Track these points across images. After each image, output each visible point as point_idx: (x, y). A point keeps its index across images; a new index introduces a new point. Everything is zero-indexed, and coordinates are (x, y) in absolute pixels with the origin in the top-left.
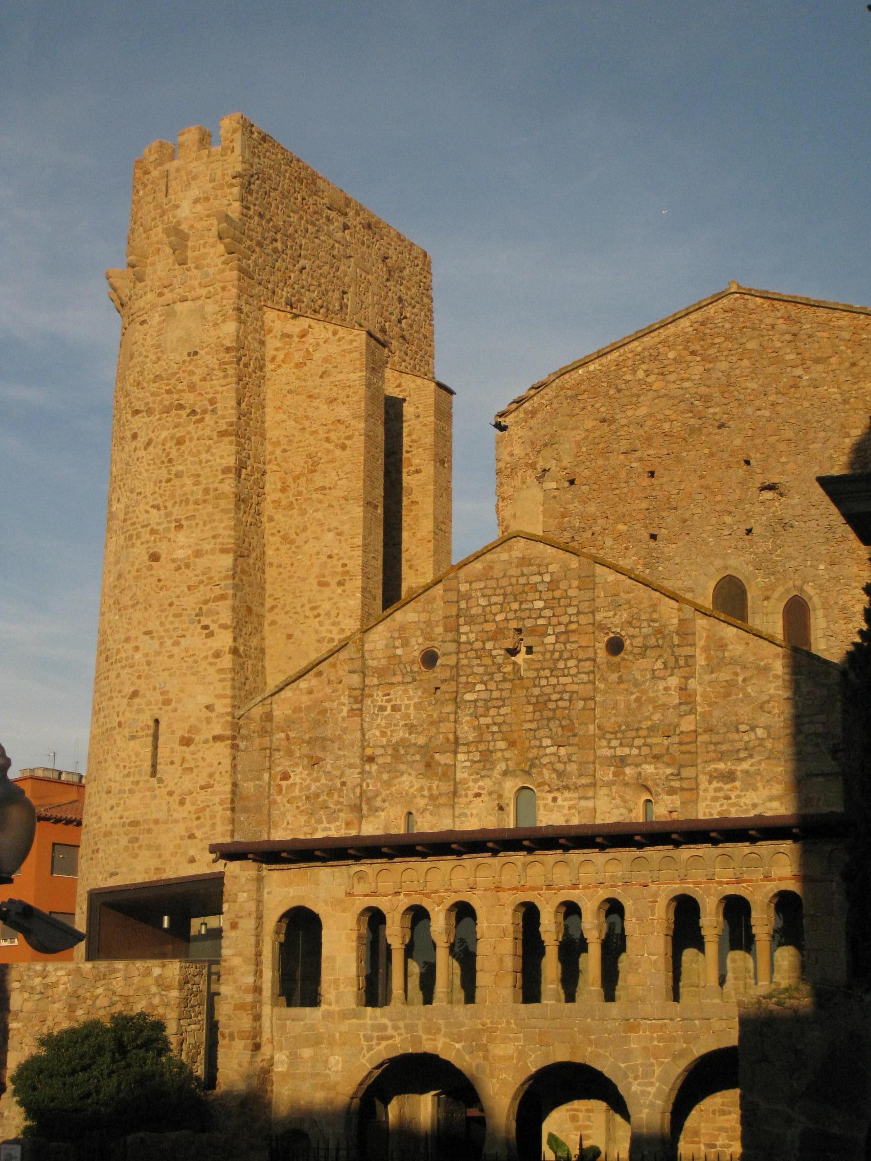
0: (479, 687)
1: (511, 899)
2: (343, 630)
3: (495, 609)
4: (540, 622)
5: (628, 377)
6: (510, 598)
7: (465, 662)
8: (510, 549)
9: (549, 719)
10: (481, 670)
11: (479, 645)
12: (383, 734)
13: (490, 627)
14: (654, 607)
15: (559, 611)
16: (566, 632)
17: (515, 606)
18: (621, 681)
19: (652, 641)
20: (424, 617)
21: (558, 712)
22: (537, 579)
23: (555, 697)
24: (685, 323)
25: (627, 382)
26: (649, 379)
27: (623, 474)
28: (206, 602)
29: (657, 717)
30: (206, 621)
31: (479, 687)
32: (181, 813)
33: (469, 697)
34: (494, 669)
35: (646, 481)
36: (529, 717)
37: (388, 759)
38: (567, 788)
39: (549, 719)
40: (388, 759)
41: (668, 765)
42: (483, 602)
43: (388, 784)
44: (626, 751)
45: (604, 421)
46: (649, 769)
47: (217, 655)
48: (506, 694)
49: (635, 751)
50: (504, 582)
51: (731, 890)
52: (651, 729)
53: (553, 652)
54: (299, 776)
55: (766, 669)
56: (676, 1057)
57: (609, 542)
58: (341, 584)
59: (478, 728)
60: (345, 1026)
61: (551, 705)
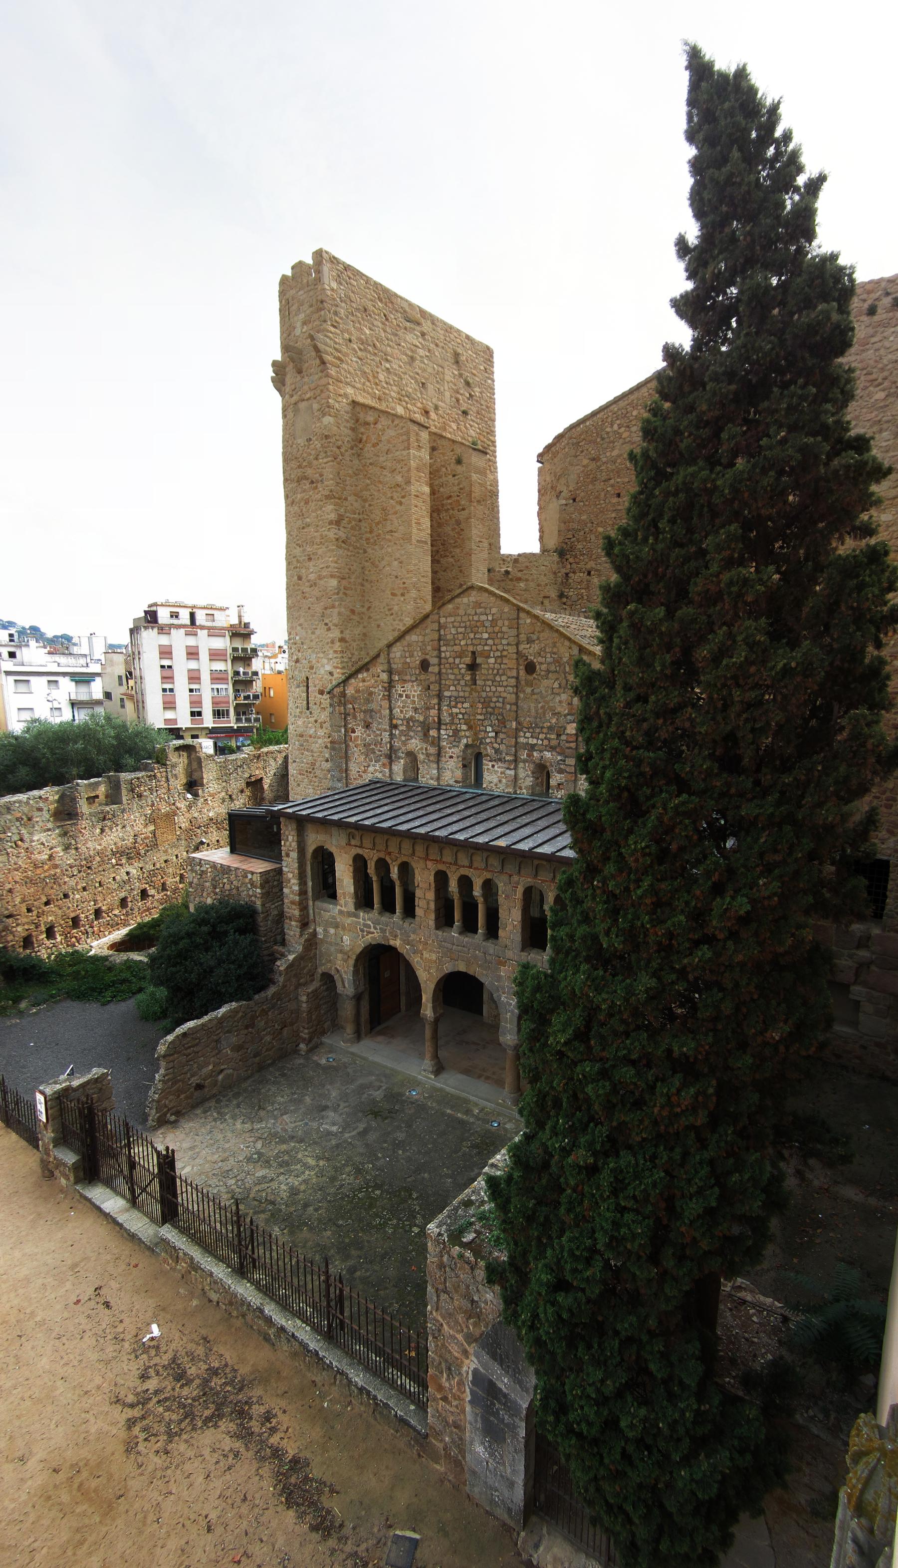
0: (452, 688)
1: (433, 867)
3: (461, 636)
4: (486, 648)
5: (608, 429)
6: (469, 630)
7: (444, 671)
8: (469, 596)
9: (491, 714)
10: (452, 677)
11: (451, 660)
12: (401, 712)
13: (457, 648)
14: (554, 645)
15: (497, 641)
16: (502, 657)
17: (472, 636)
18: (533, 693)
19: (553, 668)
20: (421, 638)
21: (496, 711)
22: (483, 618)
23: (494, 699)
24: (644, 390)
25: (608, 433)
26: (623, 429)
27: (603, 494)
28: (326, 608)
29: (554, 721)
30: (327, 621)
31: (452, 688)
32: (321, 733)
33: (447, 694)
34: (459, 677)
35: (615, 500)
36: (479, 711)
37: (404, 728)
38: (500, 760)
39: (491, 714)
40: (404, 728)
41: (559, 754)
42: (453, 631)
43: (404, 743)
44: (535, 741)
45: (593, 459)
46: (548, 755)
47: (333, 642)
48: (467, 694)
49: (540, 742)
50: (465, 619)
52: (550, 728)
53: (493, 669)
54: (359, 732)
57: (593, 537)
58: (403, 595)
59: (451, 715)
60: (350, 920)
61: (492, 705)
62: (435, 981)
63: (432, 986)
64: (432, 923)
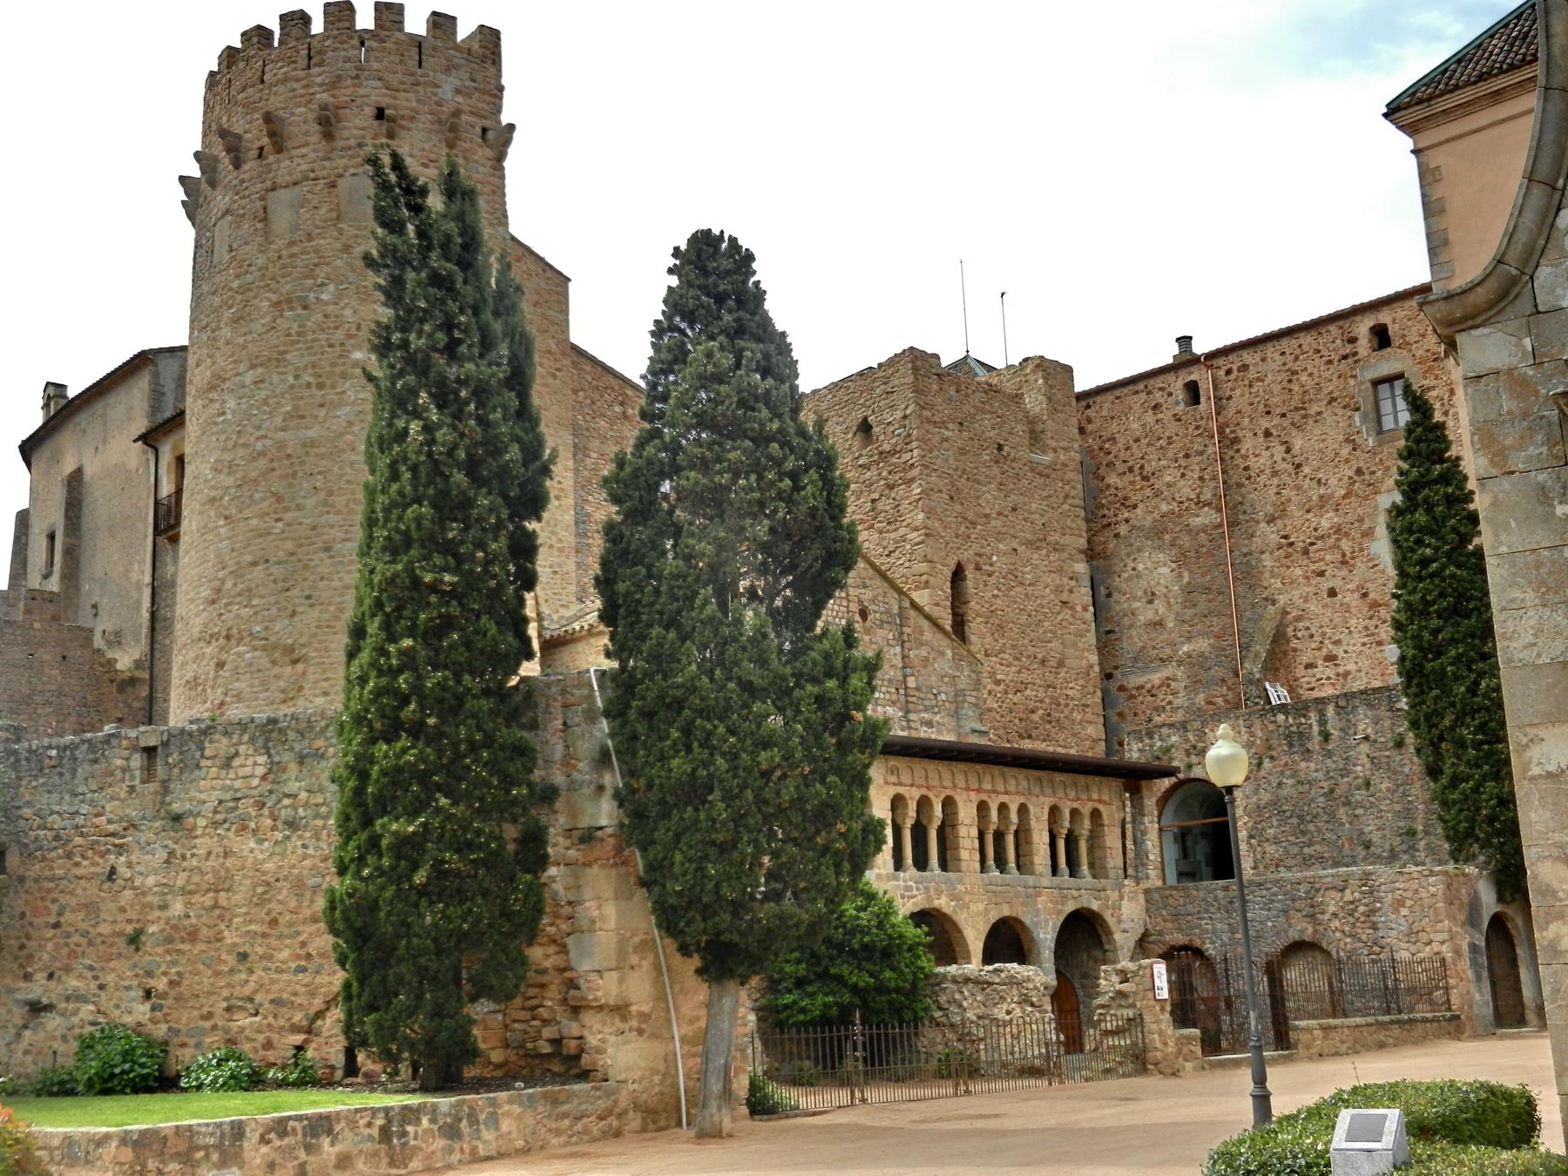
2: (560, 541)
46: (890, 710)
51: (1075, 805)
52: (890, 681)
55: (942, 654)
56: (1059, 913)
62: (983, 938)
63: (981, 945)
64: (978, 865)
